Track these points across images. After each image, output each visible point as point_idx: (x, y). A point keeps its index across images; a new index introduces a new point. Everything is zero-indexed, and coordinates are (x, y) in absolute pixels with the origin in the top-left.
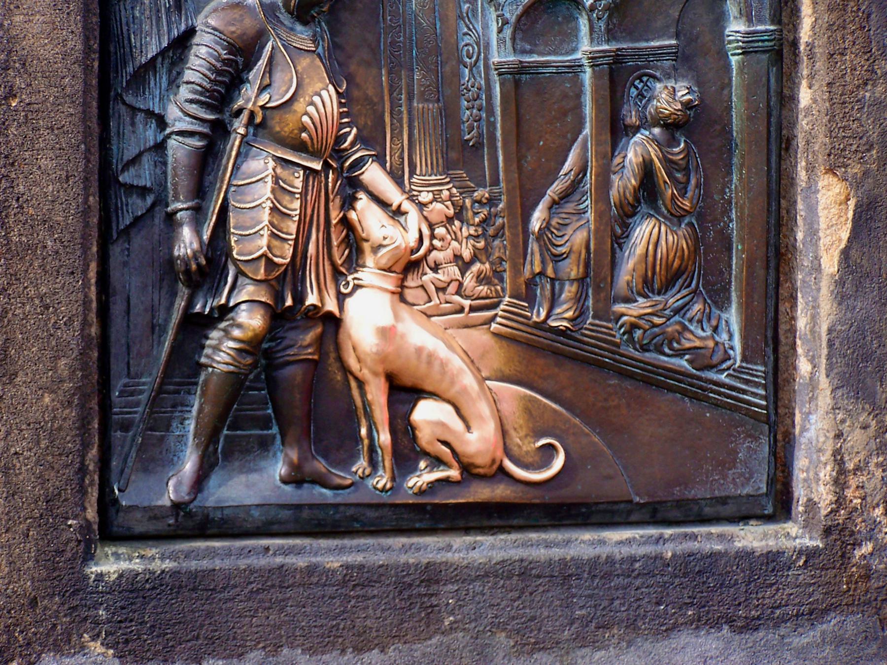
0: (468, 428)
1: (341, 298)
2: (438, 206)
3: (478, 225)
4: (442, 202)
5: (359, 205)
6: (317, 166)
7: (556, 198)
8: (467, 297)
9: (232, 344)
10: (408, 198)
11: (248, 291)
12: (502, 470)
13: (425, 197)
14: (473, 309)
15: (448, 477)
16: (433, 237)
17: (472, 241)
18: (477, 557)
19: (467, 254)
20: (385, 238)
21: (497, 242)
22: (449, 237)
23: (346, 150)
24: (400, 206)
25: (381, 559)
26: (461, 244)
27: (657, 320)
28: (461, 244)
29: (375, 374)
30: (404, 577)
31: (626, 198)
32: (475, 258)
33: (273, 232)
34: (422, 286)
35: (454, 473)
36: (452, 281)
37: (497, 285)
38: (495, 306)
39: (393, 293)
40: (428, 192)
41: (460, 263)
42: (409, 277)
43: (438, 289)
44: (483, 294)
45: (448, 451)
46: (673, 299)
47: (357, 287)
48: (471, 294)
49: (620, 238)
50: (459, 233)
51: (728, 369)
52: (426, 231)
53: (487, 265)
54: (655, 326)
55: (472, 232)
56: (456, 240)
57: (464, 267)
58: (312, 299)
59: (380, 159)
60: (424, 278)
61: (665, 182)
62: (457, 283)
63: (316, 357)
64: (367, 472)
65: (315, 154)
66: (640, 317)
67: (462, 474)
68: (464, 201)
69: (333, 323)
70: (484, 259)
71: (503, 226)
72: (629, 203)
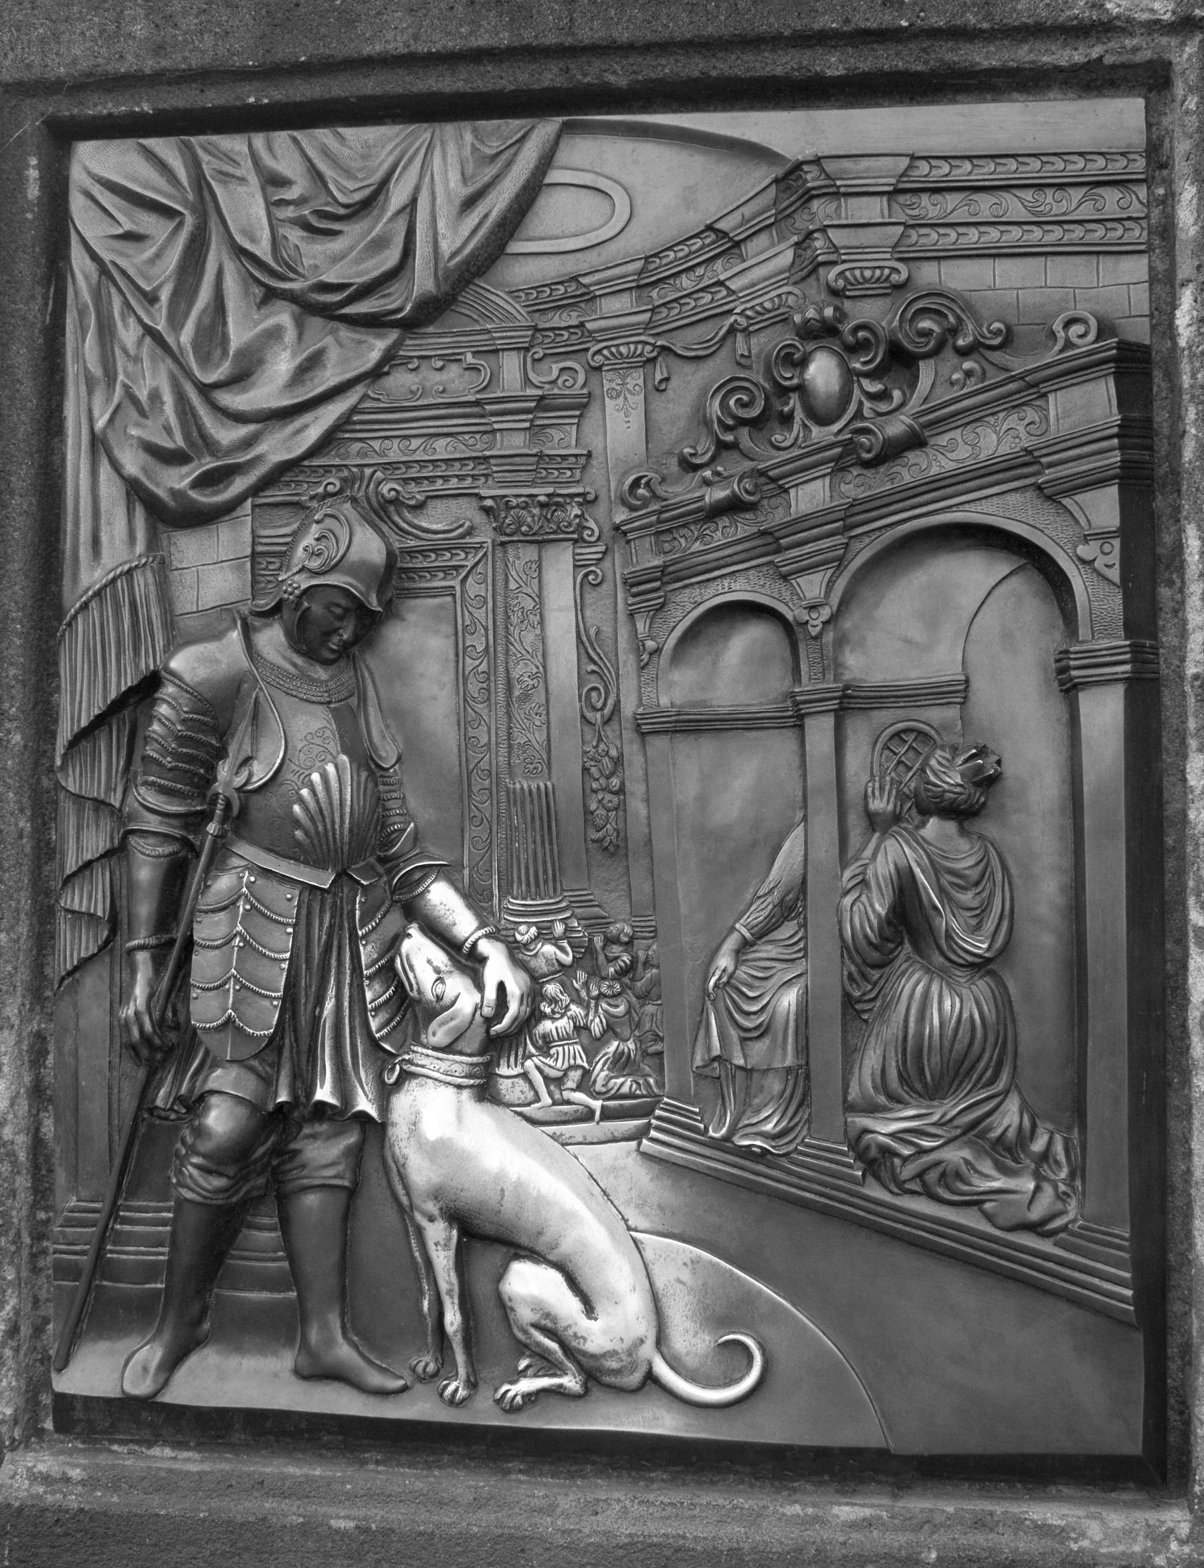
0: (589, 1309)
1: (385, 1094)
2: (549, 949)
3: (613, 979)
4: (555, 941)
5: (406, 946)
6: (324, 879)
7: (747, 935)
8: (595, 1095)
9: (195, 1160)
10: (487, 936)
11: (219, 1078)
12: (651, 1378)
13: (526, 933)
14: (607, 1115)
15: (561, 1386)
16: (534, 995)
17: (605, 1006)
18: (592, 1528)
19: (596, 1028)
20: (439, 998)
21: (650, 1009)
22: (565, 999)
23: (396, 857)
24: (474, 945)
25: (425, 1519)
26: (587, 1008)
27: (926, 1144)
28: (587, 1008)
29: (431, 1219)
30: (459, 1554)
31: (866, 937)
32: (610, 1030)
33: (243, 986)
34: (525, 1076)
35: (570, 1382)
36: (570, 1068)
37: (650, 1076)
38: (647, 1111)
39: (459, 1087)
40: (529, 924)
41: (585, 1040)
42: (503, 1062)
43: (547, 1079)
44: (625, 1089)
45: (553, 1345)
46: (951, 1107)
47: (405, 1076)
48: (604, 1090)
49: (859, 1001)
50: (583, 994)
51: (1064, 1228)
52: (514, 990)
53: (631, 1045)
54: (923, 1151)
55: (604, 989)
56: (578, 1000)
57: (593, 1047)
58: (324, 1093)
59: (448, 873)
60: (529, 1063)
61: (936, 908)
62: (579, 1072)
63: (346, 1183)
64: (431, 1368)
65: (319, 864)
66: (892, 1135)
67: (585, 1385)
68: (591, 941)
69: (374, 1130)
70: (627, 1033)
71: (656, 982)
72: (870, 943)
